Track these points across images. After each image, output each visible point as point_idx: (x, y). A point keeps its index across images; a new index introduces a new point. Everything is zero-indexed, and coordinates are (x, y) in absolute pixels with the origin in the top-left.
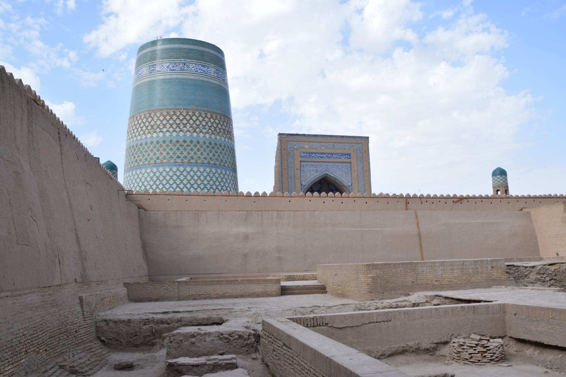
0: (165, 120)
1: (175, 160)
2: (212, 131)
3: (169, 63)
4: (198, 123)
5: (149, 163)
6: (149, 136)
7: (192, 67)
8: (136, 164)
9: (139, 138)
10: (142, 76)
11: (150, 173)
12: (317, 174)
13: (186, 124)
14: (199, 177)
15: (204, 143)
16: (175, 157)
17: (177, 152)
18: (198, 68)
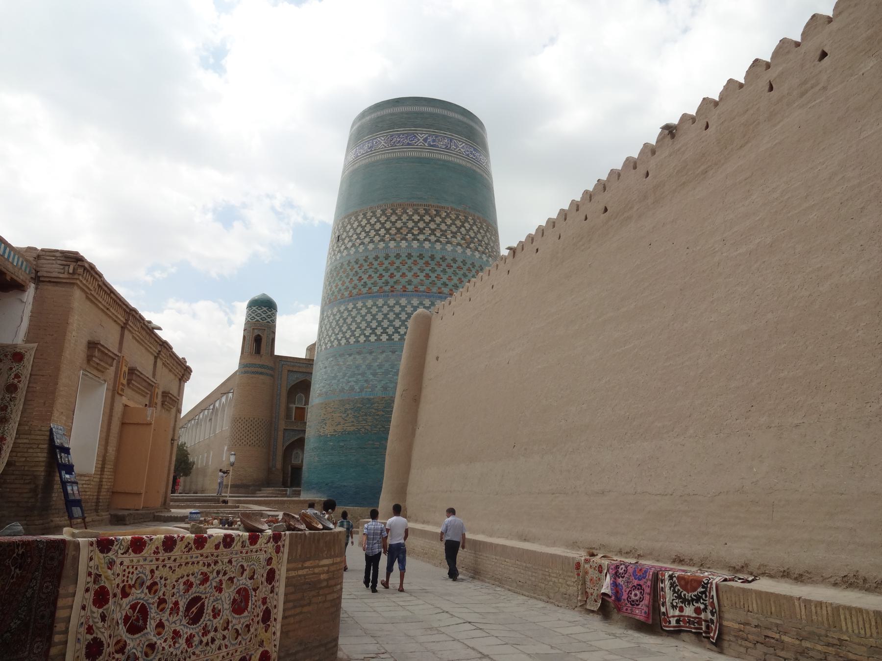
0: (422, 222)
1: (439, 288)
2: (489, 252)
3: (427, 135)
4: (472, 234)
5: (392, 289)
6: (392, 244)
7: (462, 148)
9: (371, 246)
10: (375, 150)
11: (394, 307)
13: (456, 233)
16: (439, 284)
17: (442, 275)
18: (469, 150)
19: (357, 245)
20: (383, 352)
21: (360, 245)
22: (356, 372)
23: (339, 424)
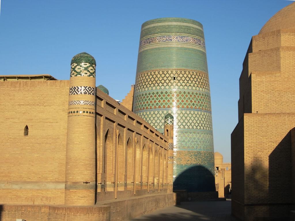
8: (194, 107)
10: (189, 42)
19: (188, 86)
20: (202, 134)
21: (189, 86)
22: (194, 140)
23: (189, 160)
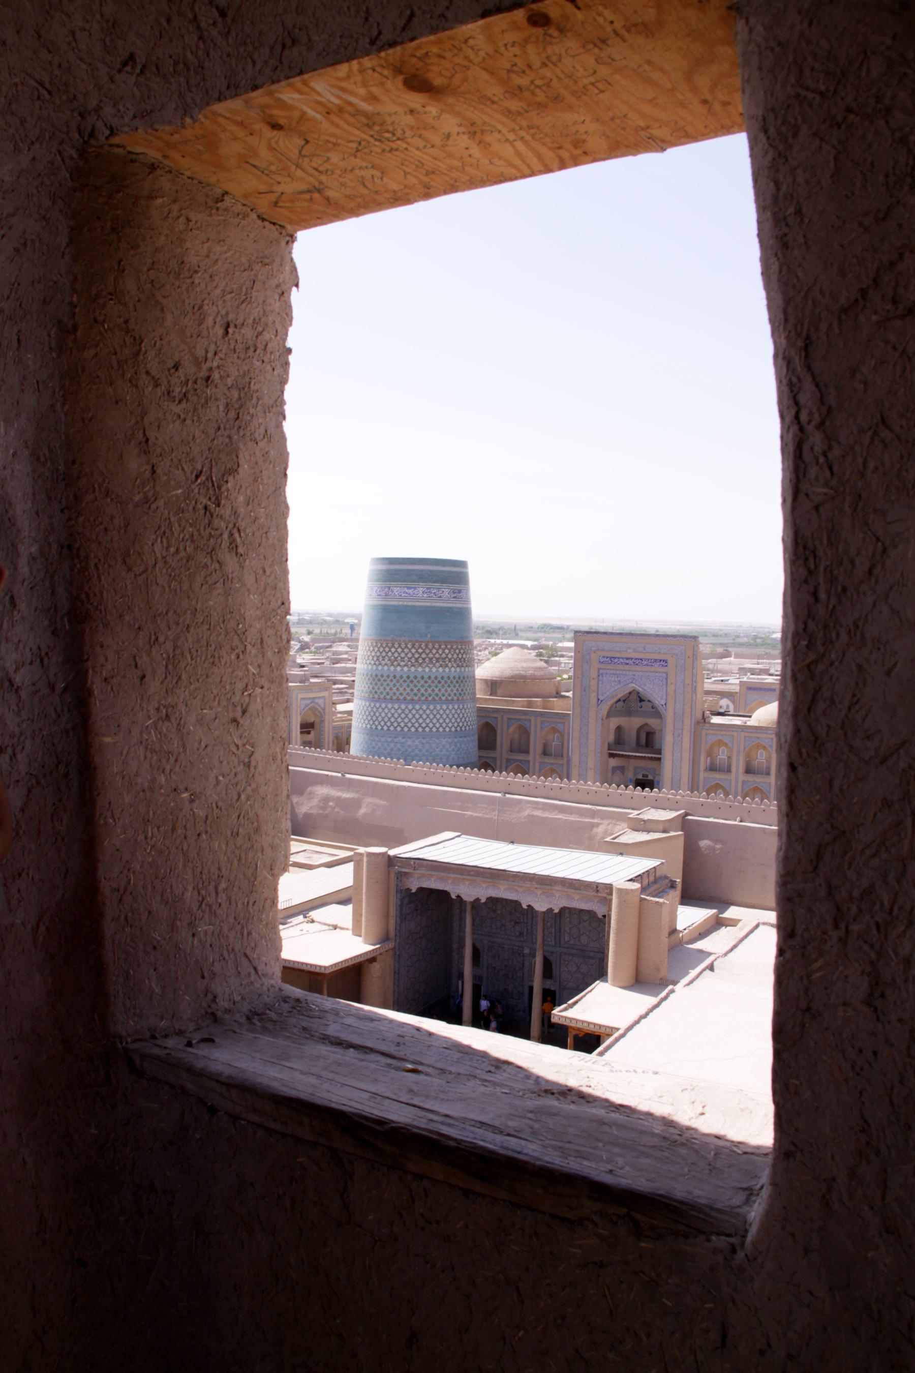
4: (396, 655)
12: (619, 686)
14: (393, 714)
15: (401, 677)
